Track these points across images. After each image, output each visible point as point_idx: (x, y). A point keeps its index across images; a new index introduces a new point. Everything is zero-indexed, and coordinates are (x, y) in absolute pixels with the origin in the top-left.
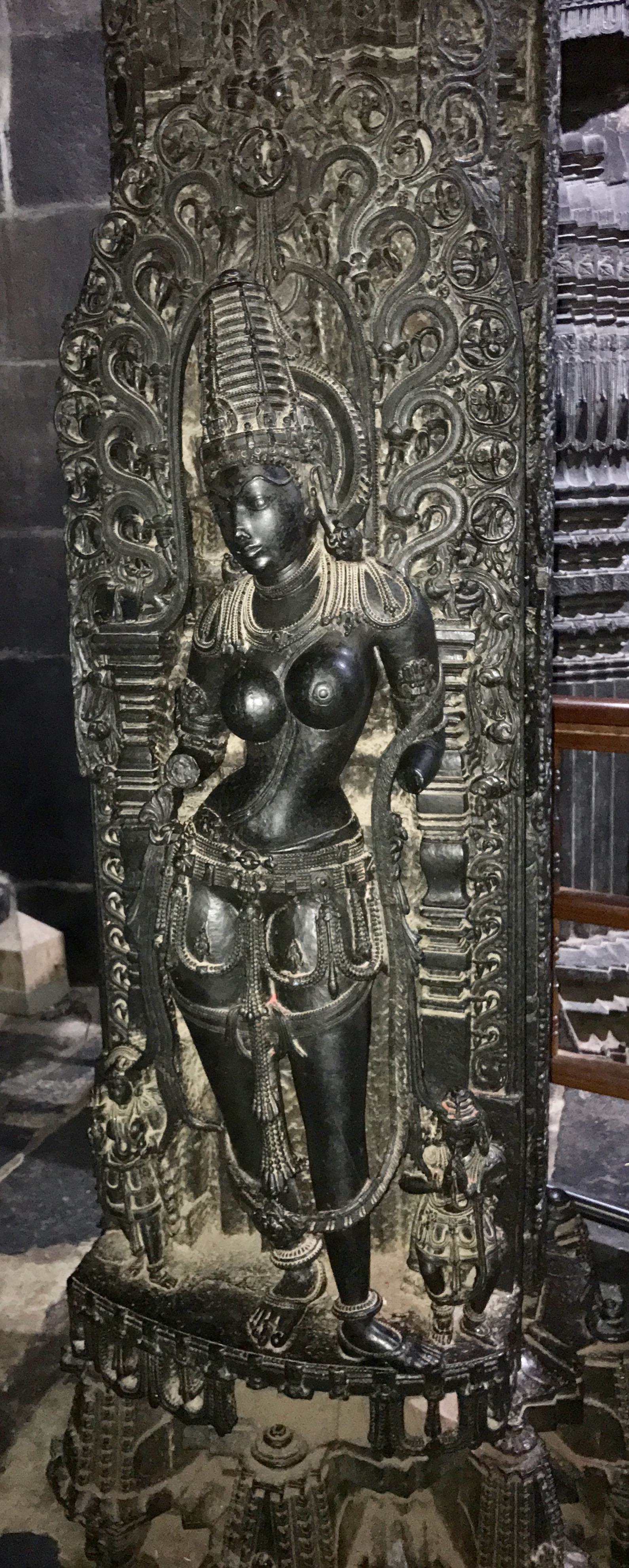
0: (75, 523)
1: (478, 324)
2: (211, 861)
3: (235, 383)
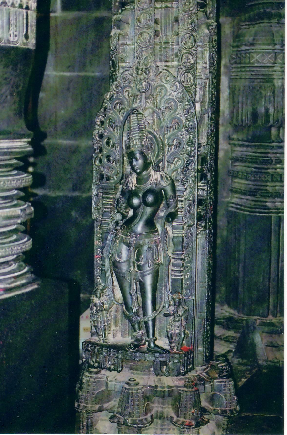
0: (96, 158)
1: (188, 123)
2: (123, 236)
3: (134, 134)
